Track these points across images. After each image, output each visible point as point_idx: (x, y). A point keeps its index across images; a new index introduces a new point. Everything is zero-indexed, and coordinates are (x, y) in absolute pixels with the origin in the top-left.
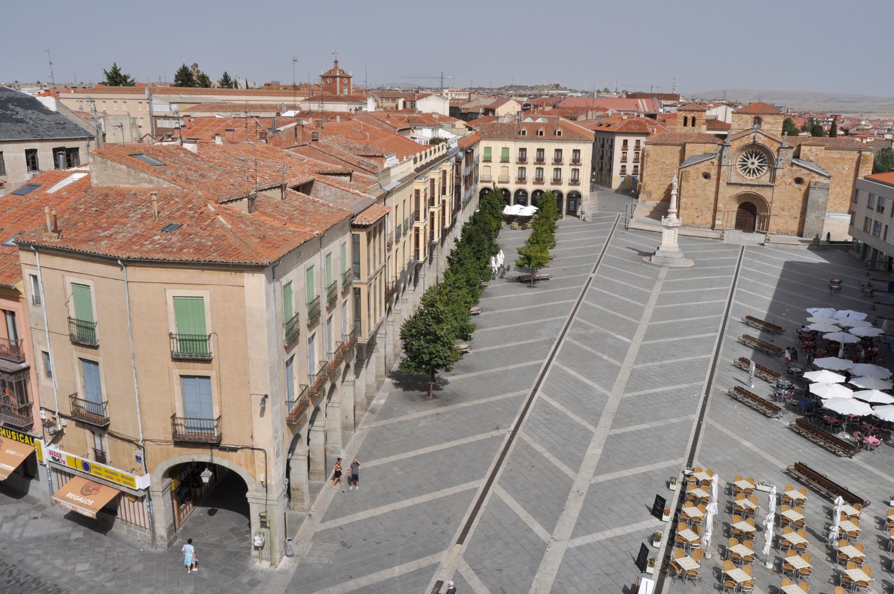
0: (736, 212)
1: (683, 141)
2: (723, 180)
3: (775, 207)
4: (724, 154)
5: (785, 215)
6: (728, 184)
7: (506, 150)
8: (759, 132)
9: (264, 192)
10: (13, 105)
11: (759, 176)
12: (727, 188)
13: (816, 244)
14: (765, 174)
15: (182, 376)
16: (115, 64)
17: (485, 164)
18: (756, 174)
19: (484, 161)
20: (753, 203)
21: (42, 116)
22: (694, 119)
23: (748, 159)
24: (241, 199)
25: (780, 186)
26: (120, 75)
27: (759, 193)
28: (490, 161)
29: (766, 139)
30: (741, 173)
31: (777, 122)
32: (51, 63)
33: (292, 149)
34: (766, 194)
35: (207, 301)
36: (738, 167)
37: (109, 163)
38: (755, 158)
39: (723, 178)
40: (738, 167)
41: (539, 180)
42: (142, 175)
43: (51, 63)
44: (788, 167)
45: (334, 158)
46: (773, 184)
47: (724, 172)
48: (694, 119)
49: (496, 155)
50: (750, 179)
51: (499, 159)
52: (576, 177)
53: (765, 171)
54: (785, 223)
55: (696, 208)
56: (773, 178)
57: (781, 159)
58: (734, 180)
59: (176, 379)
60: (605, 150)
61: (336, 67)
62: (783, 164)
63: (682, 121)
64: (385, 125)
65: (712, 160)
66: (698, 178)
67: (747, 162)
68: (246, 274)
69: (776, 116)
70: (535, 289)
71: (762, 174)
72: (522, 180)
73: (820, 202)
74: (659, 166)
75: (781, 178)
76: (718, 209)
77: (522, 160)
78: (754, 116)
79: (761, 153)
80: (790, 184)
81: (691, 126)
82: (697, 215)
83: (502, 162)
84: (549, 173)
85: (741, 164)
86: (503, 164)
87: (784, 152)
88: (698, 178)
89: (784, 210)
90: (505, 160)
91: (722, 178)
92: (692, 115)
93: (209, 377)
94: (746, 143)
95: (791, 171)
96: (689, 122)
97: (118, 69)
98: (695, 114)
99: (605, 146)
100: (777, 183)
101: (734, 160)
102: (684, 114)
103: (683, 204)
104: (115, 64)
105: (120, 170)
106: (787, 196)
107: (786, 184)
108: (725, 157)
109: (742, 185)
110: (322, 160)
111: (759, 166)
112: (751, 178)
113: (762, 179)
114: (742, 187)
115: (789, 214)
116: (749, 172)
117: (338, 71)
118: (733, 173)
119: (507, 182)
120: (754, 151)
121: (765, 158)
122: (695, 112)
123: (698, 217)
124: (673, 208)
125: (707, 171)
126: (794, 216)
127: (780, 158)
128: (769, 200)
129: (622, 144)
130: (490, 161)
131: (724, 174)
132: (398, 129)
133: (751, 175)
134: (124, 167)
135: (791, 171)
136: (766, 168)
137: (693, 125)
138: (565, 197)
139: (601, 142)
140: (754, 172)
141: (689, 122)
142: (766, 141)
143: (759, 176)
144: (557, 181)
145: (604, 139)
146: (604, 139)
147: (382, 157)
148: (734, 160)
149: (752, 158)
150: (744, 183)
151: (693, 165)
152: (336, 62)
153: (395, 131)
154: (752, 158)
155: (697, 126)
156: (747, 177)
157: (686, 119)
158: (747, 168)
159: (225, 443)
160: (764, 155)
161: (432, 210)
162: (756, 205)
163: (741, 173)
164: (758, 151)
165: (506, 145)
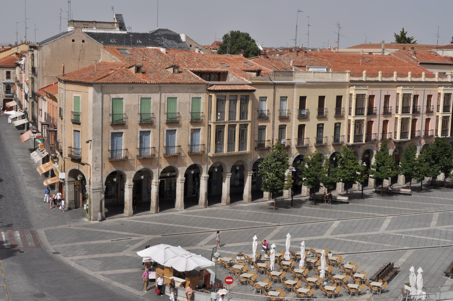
9: (168, 70)
10: (165, 38)
15: (75, 131)
16: (403, 29)
21: (175, 43)
24: (133, 66)
26: (405, 37)
32: (309, 25)
33: (252, 60)
35: (81, 98)
37: (106, 51)
42: (113, 57)
43: (309, 25)
45: (270, 65)
59: (73, 131)
64: (411, 59)
68: (89, 87)
93: (79, 131)
97: (405, 33)
104: (403, 29)
105: (108, 54)
110: (265, 66)
132: (419, 63)
134: (109, 53)
147: (305, 67)
153: (417, 63)
159: (83, 161)
161: (396, 116)
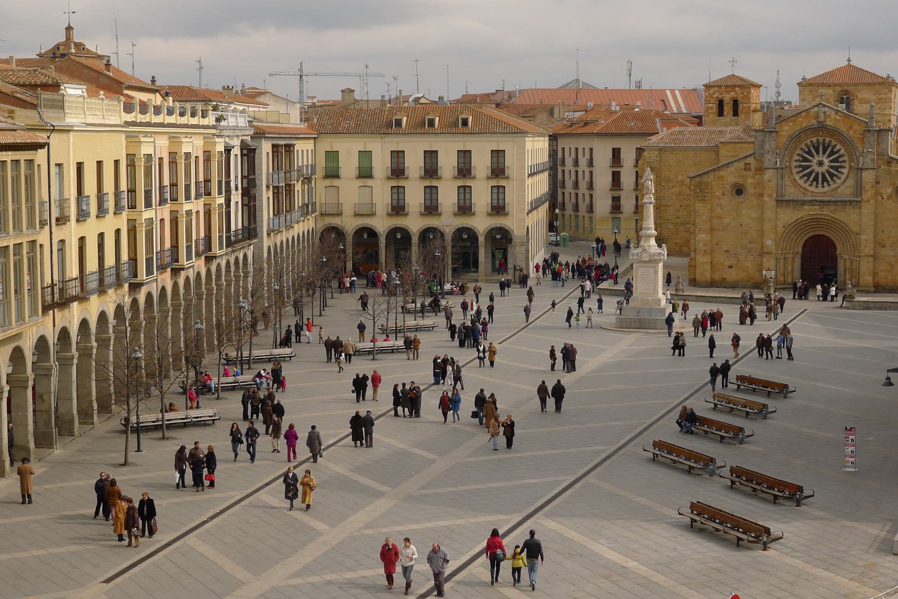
0: (799, 255)
2: (769, 196)
3: (867, 240)
7: (365, 156)
8: (824, 106)
11: (833, 186)
14: (845, 181)
17: (328, 182)
18: (828, 182)
19: (327, 177)
20: (830, 236)
22: (736, 103)
23: (812, 156)
28: (337, 176)
29: (838, 118)
30: (801, 182)
31: (881, 99)
34: (847, 216)
36: (795, 171)
38: (824, 153)
39: (769, 192)
40: (795, 171)
41: (431, 208)
44: (882, 167)
47: (769, 181)
48: (736, 103)
49: (349, 165)
50: (820, 191)
51: (355, 173)
52: (501, 201)
53: (843, 177)
55: (727, 251)
56: (859, 188)
58: (791, 193)
60: (580, 170)
61: (68, 38)
65: (749, 160)
66: (724, 194)
67: (810, 161)
69: (878, 87)
70: (381, 361)
72: (398, 209)
74: (673, 190)
77: (398, 172)
78: (838, 89)
79: (833, 143)
80: (889, 198)
81: (732, 116)
82: (727, 263)
83: (360, 177)
84: (448, 197)
85: (800, 166)
86: (361, 182)
88: (724, 194)
89: (884, 246)
90: (365, 173)
92: (733, 94)
94: (804, 125)
95: (889, 173)
96: (728, 109)
99: (580, 163)
102: (717, 94)
103: (701, 245)
107: (883, 198)
109: (803, 203)
111: (831, 167)
112: (820, 189)
113: (839, 190)
114: (805, 207)
115: (893, 253)
116: (816, 179)
117: (73, 46)
118: (787, 182)
119: (372, 215)
120: (821, 140)
121: (842, 152)
123: (730, 267)
124: (649, 229)
125: (740, 181)
128: (855, 229)
129: (611, 156)
130: (337, 176)
133: (820, 185)
135: (889, 173)
136: (845, 171)
137: (736, 113)
138: (481, 239)
139: (573, 156)
140: (824, 179)
141: (728, 109)
142: (837, 121)
143: (833, 186)
144: (465, 209)
145: (577, 149)
146: (577, 149)
149: (818, 153)
151: (714, 170)
152: (69, 29)
154: (818, 153)
155: (742, 116)
156: (812, 189)
157: (721, 103)
158: (812, 172)
160: (838, 147)
162: (834, 240)
163: (801, 182)
164: (828, 140)
165: (365, 147)
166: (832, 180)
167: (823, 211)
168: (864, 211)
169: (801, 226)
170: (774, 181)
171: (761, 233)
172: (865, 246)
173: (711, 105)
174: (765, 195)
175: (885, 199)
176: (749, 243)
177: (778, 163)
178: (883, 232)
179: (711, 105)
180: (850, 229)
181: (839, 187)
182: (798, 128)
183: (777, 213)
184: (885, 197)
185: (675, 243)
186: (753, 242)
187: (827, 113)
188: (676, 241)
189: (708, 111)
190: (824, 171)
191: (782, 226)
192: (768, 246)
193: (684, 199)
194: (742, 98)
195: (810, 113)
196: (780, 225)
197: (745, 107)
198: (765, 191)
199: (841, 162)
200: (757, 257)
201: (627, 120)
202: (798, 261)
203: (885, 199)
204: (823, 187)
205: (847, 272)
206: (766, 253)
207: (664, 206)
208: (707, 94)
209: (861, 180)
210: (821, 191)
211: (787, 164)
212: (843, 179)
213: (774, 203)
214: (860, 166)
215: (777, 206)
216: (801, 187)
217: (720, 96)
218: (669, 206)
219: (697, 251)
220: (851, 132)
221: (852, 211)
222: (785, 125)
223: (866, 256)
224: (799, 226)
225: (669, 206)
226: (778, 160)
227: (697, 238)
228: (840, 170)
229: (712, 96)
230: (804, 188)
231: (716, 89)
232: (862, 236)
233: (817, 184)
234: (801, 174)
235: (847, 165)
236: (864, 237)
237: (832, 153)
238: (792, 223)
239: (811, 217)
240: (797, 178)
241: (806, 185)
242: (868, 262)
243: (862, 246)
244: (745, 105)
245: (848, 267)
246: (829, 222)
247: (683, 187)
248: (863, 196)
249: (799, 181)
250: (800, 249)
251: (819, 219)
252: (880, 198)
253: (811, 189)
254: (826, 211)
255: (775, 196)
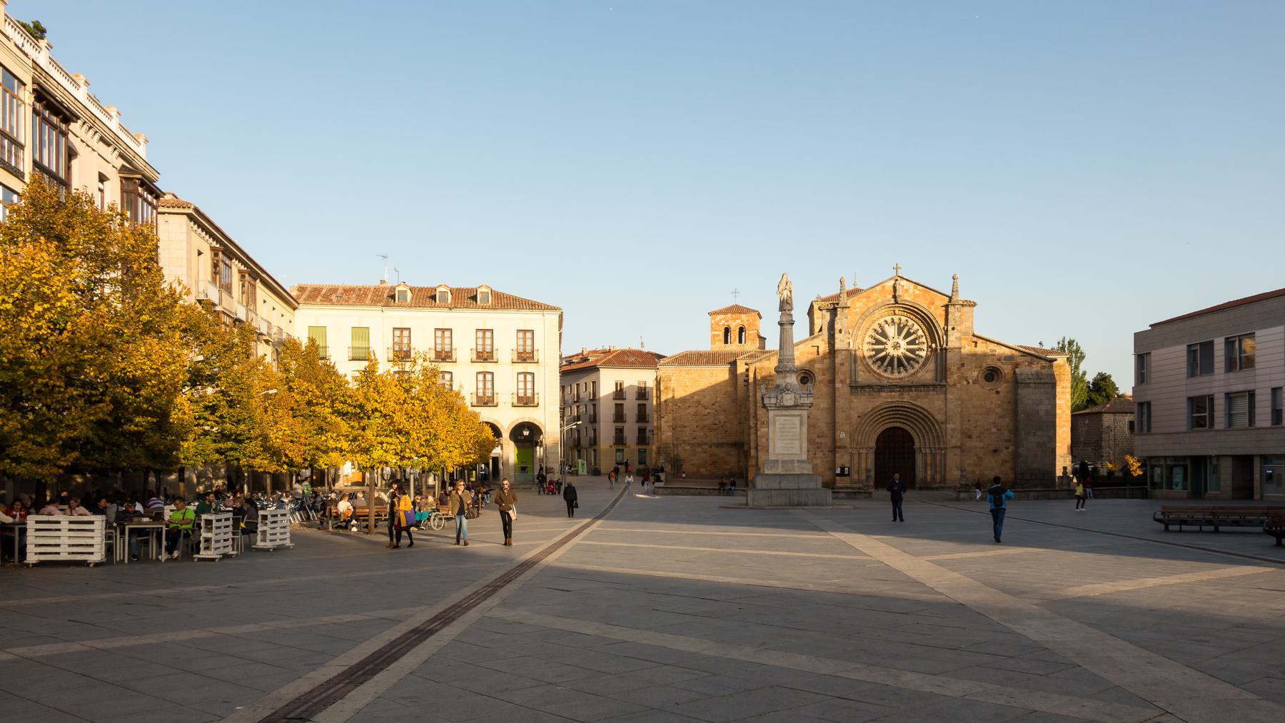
0: (873, 451)
1: (732, 360)
2: (842, 382)
3: (953, 430)
4: (837, 327)
5: (975, 447)
6: (856, 388)
12: (852, 398)
13: (1065, 488)
25: (958, 386)
27: (918, 403)
29: (917, 292)
30: (874, 368)
39: (842, 377)
46: (944, 383)
47: (842, 364)
48: (742, 330)
54: (976, 465)
57: (953, 329)
62: (960, 339)
63: (722, 334)
71: (917, 366)
73: (1042, 413)
74: (690, 410)
75: (959, 369)
76: (838, 444)
80: (975, 382)
87: (958, 314)
89: (970, 437)
91: (839, 377)
92: (739, 321)
94: (879, 300)
96: (734, 335)
98: (743, 320)
100: (951, 380)
101: (859, 340)
102: (723, 322)
106: (974, 407)
107: (969, 383)
108: (840, 331)
109: (881, 388)
112: (896, 375)
113: (919, 375)
114: (883, 394)
115: (981, 445)
122: (743, 316)
126: (992, 448)
127: (950, 328)
128: (940, 417)
131: (844, 369)
133: (896, 371)
141: (734, 335)
142: (916, 296)
148: (859, 340)
150: (885, 382)
157: (727, 330)
164: (904, 319)
166: (909, 364)
167: (903, 398)
168: (949, 396)
169: (876, 416)
170: (847, 364)
171: (833, 425)
172: (952, 437)
173: (717, 333)
174: (837, 380)
175: (971, 384)
176: (818, 437)
177: (851, 344)
178: (969, 421)
179: (717, 333)
180: (933, 417)
181: (917, 371)
182: (871, 304)
183: (851, 401)
184: (971, 381)
185: (692, 464)
186: (822, 437)
187: (905, 288)
188: (692, 462)
189: (714, 338)
190: (900, 354)
191: (857, 416)
192: (841, 439)
193: (701, 420)
194: (749, 325)
195: (886, 288)
196: (854, 414)
197: (751, 334)
198: (837, 376)
199: (918, 344)
200: (827, 453)
201: (628, 356)
202: (872, 457)
203: (971, 384)
204: (899, 372)
205: (929, 468)
206: (840, 448)
207: (680, 427)
208: (713, 322)
209: (946, 361)
210: (898, 377)
211: (860, 346)
212: (921, 363)
213: (847, 390)
214: (945, 345)
215: (852, 393)
216: (875, 372)
217: (726, 324)
218: (685, 427)
219: (759, 448)
220: (933, 308)
221: (936, 397)
222: (858, 301)
223: (953, 447)
224: (879, 413)
225: (685, 427)
226: (851, 341)
227: (759, 433)
228: (917, 352)
229: (717, 324)
230: (878, 374)
231: (722, 316)
232: (948, 426)
233: (892, 369)
234: (874, 359)
235: (925, 347)
236: (950, 426)
237: (908, 334)
238: (868, 413)
239: (890, 405)
240: (870, 363)
241: (880, 371)
242: (955, 455)
243: (949, 437)
244: (751, 332)
245: (929, 462)
246: (909, 410)
247: (700, 407)
248: (948, 380)
249: (872, 367)
250: (873, 444)
251: (898, 407)
252: (965, 383)
253: (885, 375)
254: (907, 398)
255: (848, 381)
